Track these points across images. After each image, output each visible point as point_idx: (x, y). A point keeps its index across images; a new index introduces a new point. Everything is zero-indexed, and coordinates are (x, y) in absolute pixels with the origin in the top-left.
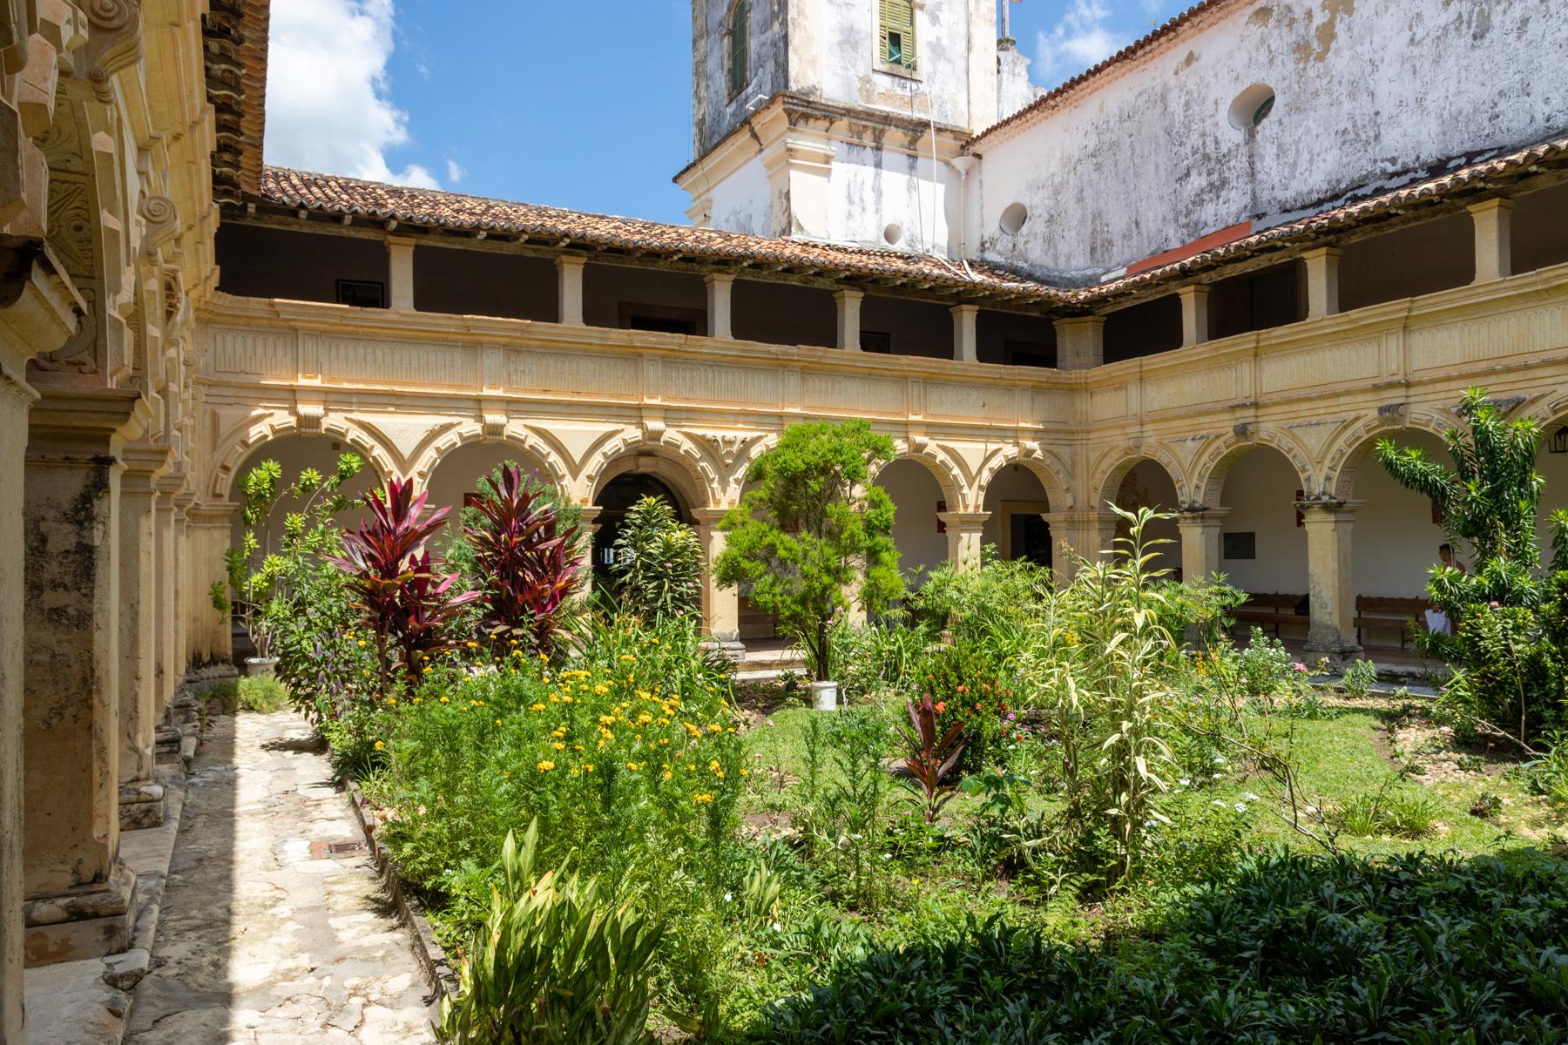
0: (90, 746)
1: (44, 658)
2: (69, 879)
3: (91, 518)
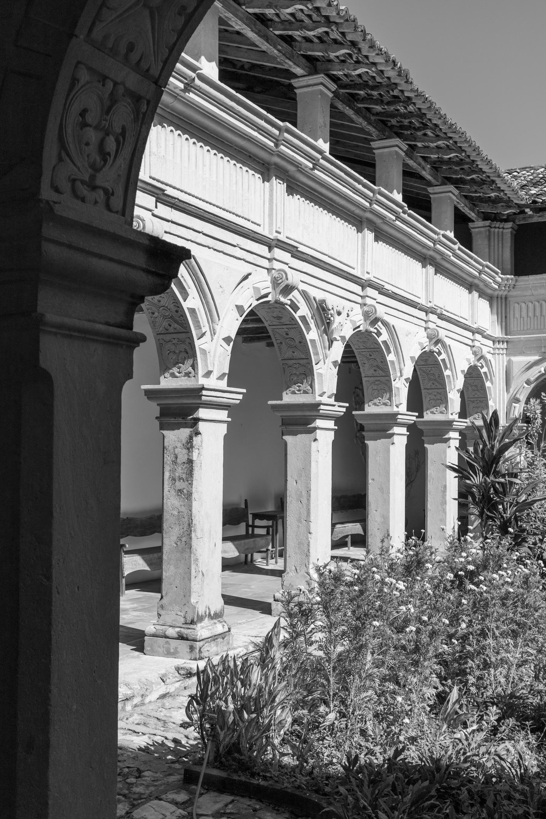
0: (190, 557)
1: (175, 513)
2: (183, 620)
3: (192, 447)
